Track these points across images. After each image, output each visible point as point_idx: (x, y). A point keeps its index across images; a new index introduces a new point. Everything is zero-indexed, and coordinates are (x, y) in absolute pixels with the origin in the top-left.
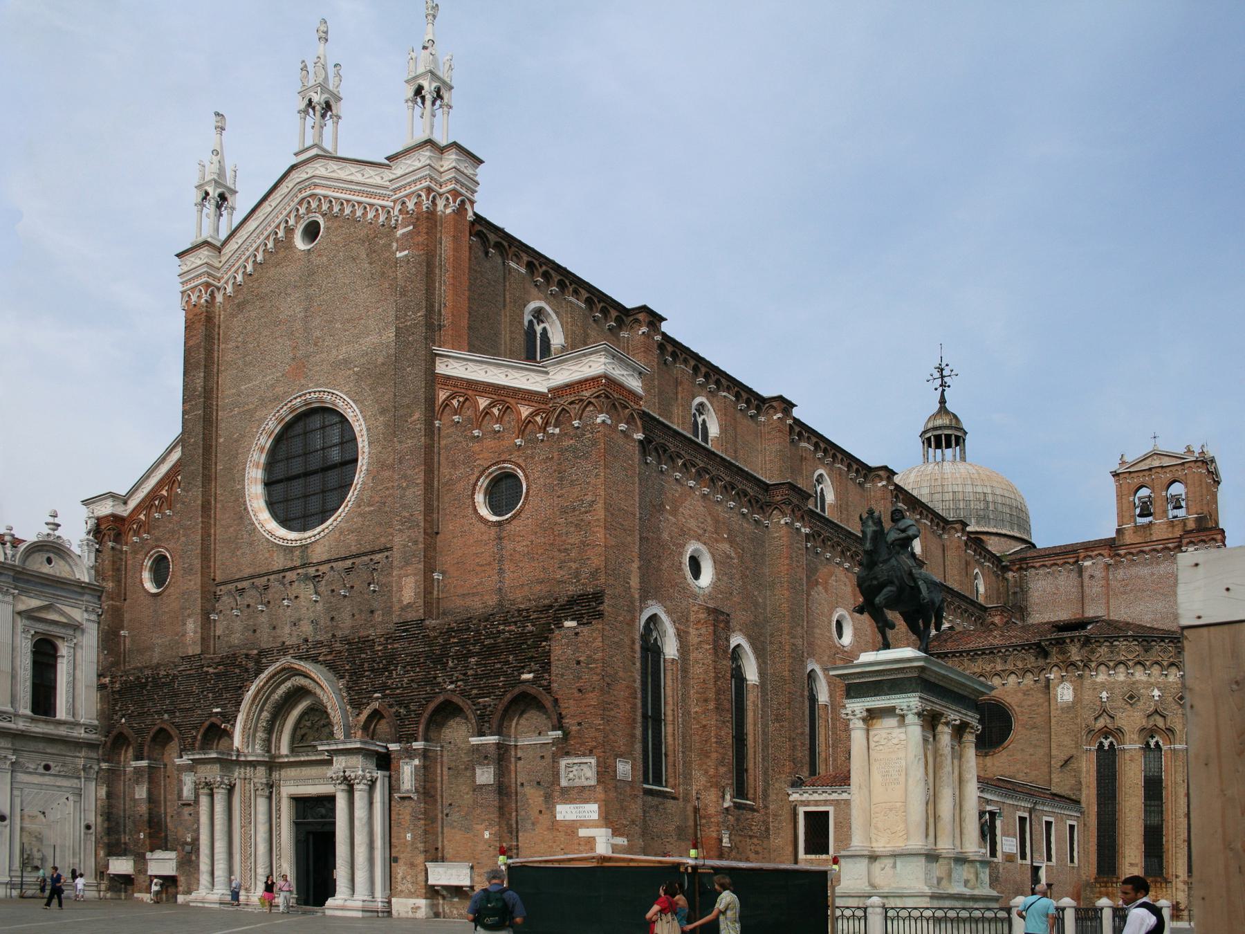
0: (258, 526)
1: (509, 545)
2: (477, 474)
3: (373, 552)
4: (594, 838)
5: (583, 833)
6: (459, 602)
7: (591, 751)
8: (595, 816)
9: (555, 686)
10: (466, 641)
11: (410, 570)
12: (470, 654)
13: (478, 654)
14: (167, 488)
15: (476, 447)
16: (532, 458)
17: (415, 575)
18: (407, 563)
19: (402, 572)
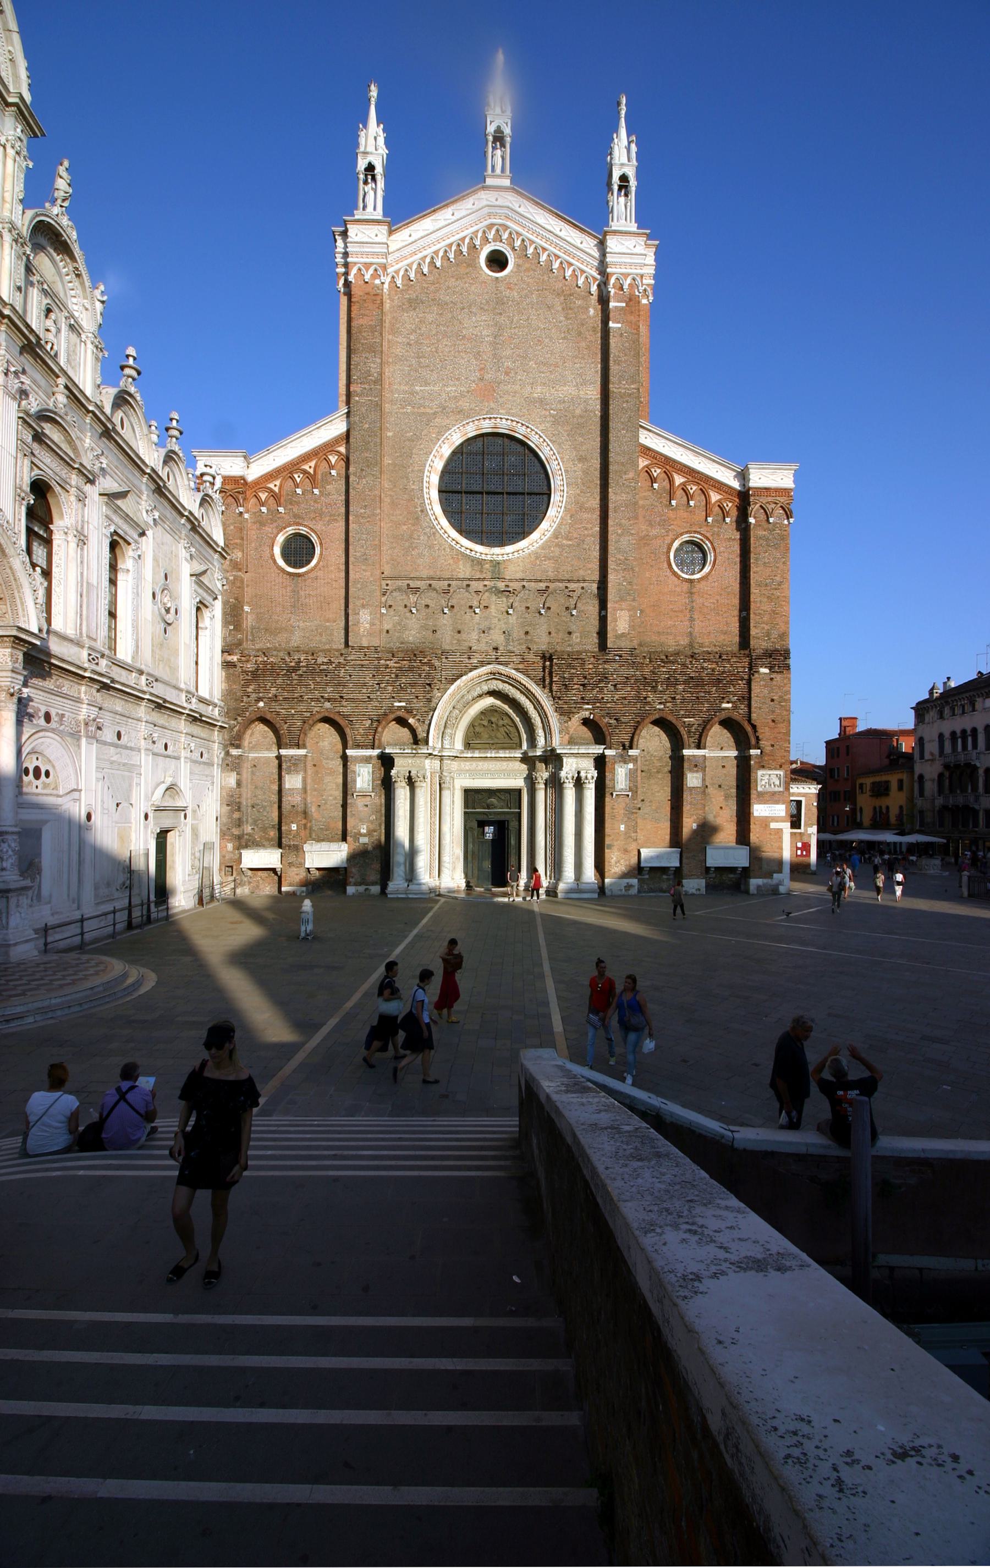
0: (441, 532)
1: (699, 600)
2: (671, 536)
3: (569, 581)
4: (782, 829)
5: (773, 825)
6: (654, 638)
7: (781, 766)
8: (783, 814)
9: (754, 716)
10: (675, 671)
11: (624, 605)
12: (676, 683)
13: (685, 682)
14: (313, 464)
15: (671, 514)
16: (719, 535)
17: (629, 610)
18: (622, 599)
19: (617, 605)
